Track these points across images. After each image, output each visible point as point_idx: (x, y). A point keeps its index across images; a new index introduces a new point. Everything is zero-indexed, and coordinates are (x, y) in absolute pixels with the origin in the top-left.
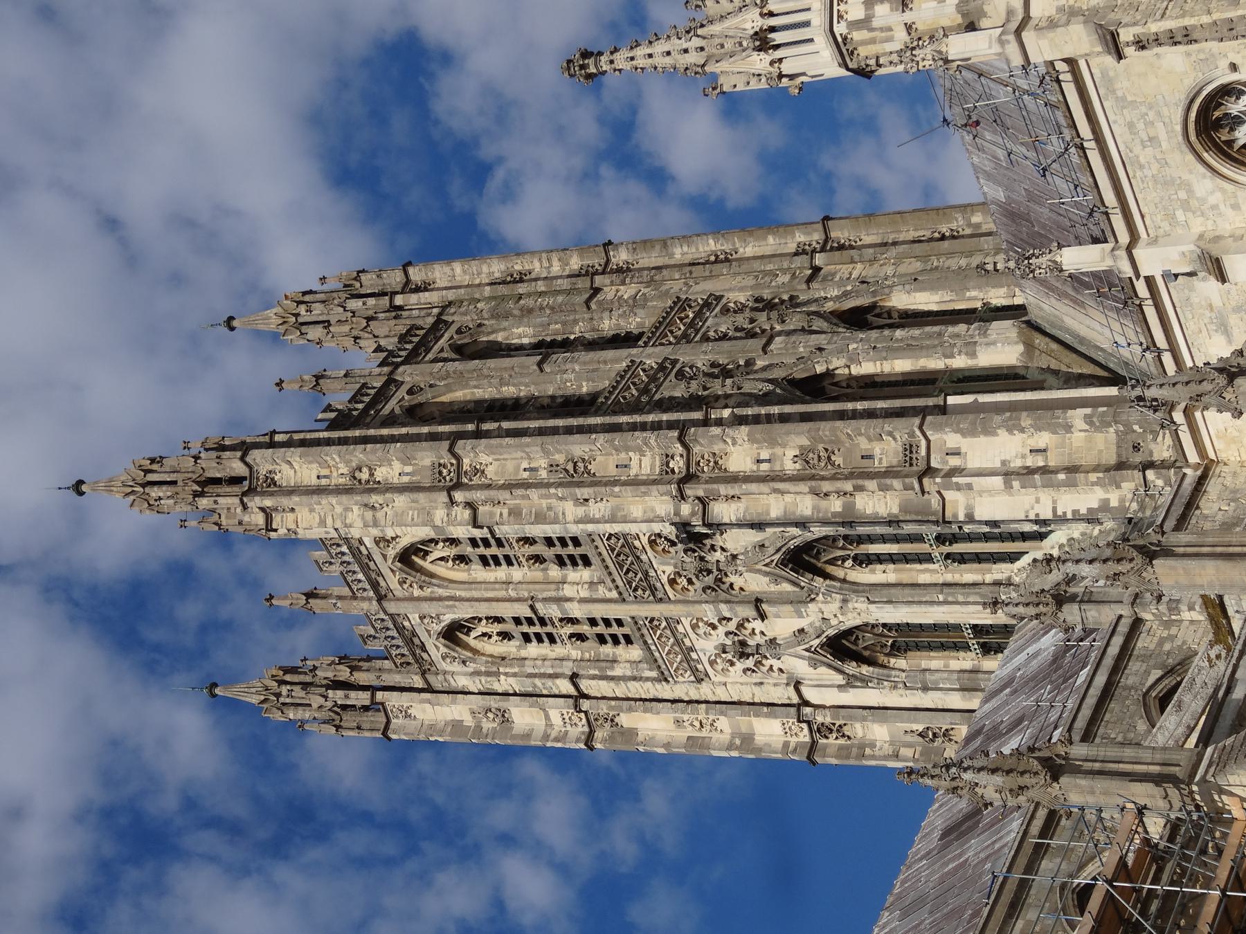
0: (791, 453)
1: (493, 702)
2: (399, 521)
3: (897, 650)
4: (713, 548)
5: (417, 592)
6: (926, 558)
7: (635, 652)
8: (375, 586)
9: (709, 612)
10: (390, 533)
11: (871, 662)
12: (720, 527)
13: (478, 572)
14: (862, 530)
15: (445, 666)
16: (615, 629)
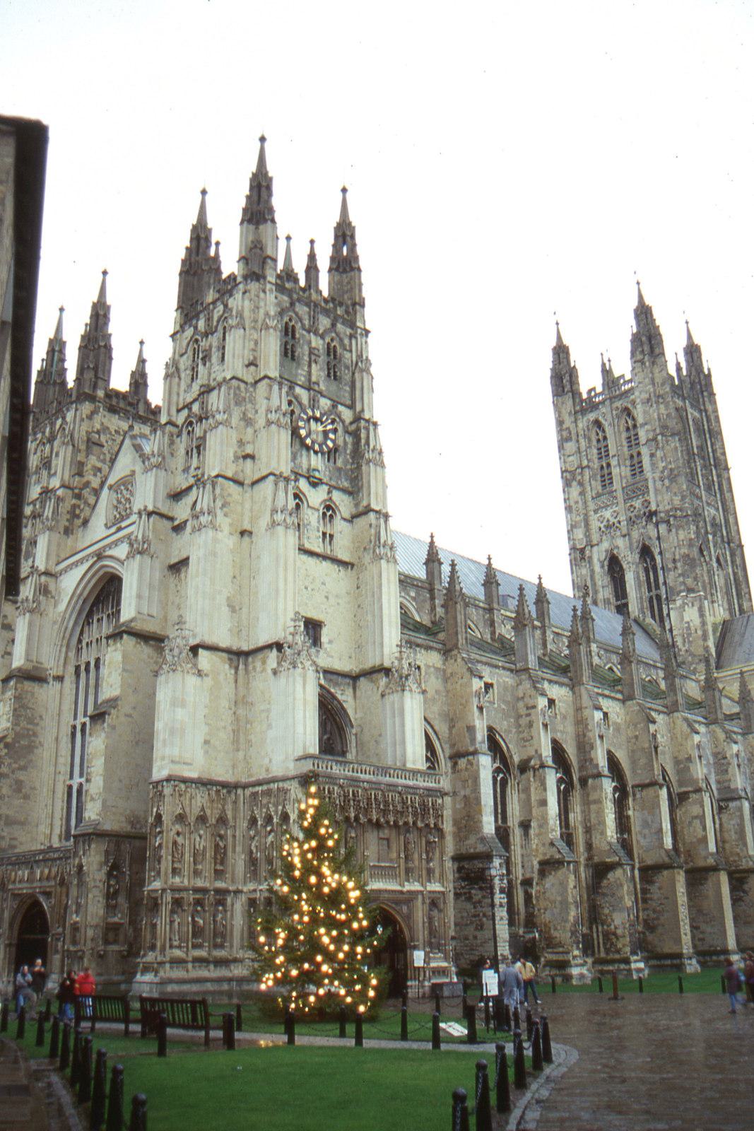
0: (686, 551)
1: (574, 437)
2: (645, 412)
3: (613, 579)
4: (646, 521)
5: (614, 412)
6: (650, 590)
7: (600, 488)
8: (615, 397)
9: (622, 518)
10: (638, 406)
11: (609, 570)
12: (657, 525)
13: (624, 435)
14: (660, 573)
15: (585, 419)
16: (607, 482)
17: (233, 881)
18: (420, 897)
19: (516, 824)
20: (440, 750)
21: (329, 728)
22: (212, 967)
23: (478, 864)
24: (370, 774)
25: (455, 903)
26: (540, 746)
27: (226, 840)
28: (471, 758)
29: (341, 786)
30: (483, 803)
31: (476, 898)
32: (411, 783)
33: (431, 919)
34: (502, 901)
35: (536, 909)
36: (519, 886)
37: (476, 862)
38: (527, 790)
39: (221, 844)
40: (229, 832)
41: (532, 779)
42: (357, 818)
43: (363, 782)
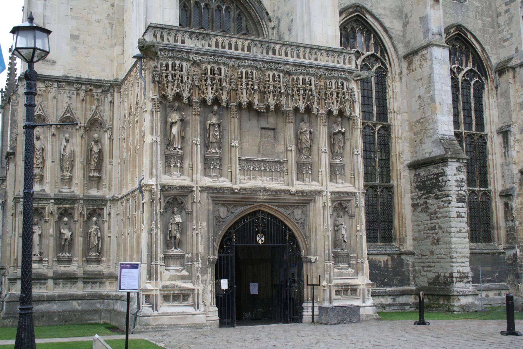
17: (110, 189)
18: (319, 202)
19: (494, 130)
20: (392, 49)
21: (244, 24)
22: (80, 284)
23: (433, 170)
24: (243, 50)
25: (413, 215)
26: (521, 44)
27: (102, 145)
28: (424, 52)
29: (195, 63)
30: (438, 100)
31: (432, 210)
32: (307, 61)
33: (336, 228)
34: (460, 210)
35: (517, 223)
36: (498, 199)
37: (431, 168)
38: (506, 94)
39: (96, 149)
40: (107, 135)
41: (511, 81)
42: (217, 101)
43: (231, 58)
